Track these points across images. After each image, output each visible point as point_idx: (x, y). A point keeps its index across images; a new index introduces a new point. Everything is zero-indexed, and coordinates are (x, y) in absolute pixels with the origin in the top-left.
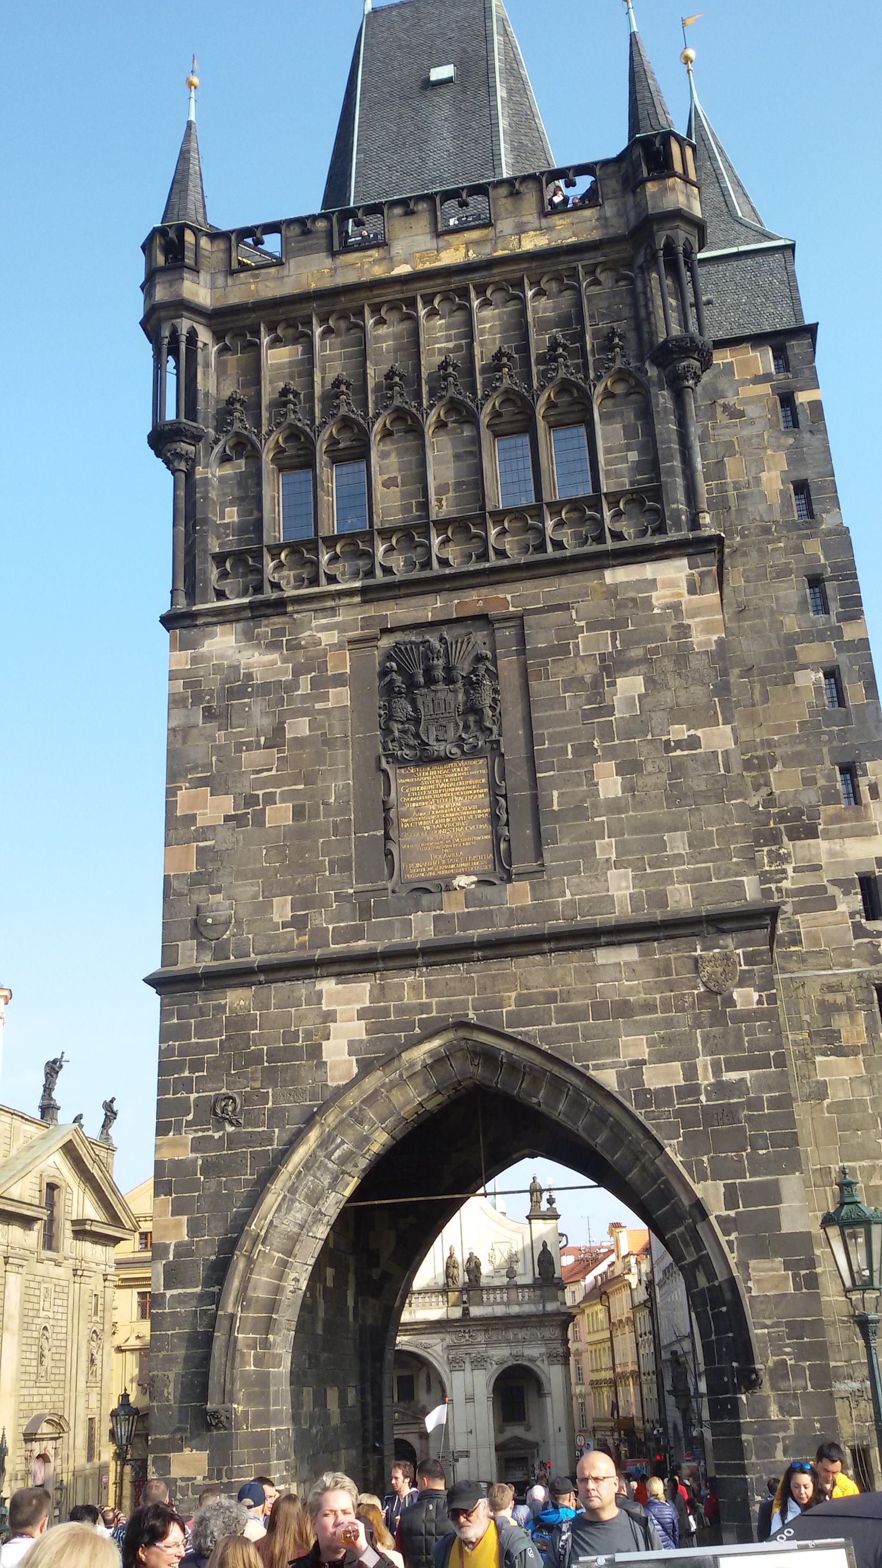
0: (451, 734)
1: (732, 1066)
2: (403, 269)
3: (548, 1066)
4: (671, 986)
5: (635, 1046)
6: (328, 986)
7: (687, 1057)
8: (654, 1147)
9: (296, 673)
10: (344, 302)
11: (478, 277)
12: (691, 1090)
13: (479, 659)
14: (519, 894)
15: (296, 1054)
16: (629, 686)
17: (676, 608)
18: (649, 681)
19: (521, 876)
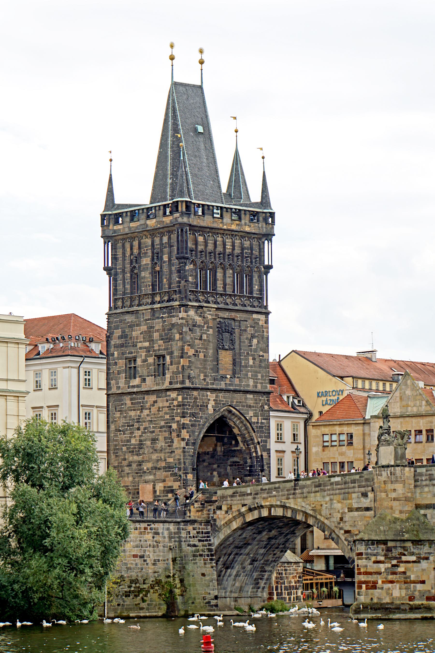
0: (228, 345)
1: (264, 419)
2: (225, 227)
3: (240, 415)
4: (257, 403)
5: (251, 413)
6: (209, 393)
7: (258, 416)
8: (253, 432)
9: (204, 324)
10: (213, 231)
11: (236, 233)
12: (258, 423)
13: (232, 329)
14: (237, 381)
15: (204, 406)
16: (255, 341)
17: (262, 326)
18: (258, 341)
19: (238, 377)
